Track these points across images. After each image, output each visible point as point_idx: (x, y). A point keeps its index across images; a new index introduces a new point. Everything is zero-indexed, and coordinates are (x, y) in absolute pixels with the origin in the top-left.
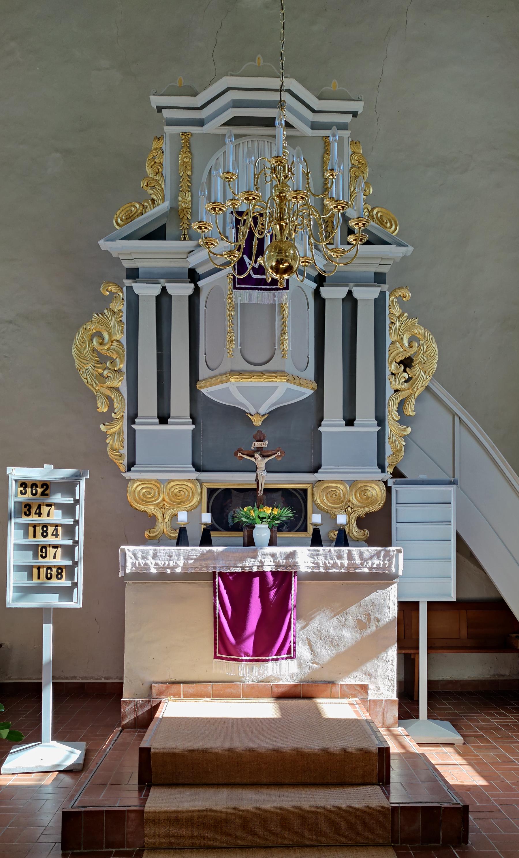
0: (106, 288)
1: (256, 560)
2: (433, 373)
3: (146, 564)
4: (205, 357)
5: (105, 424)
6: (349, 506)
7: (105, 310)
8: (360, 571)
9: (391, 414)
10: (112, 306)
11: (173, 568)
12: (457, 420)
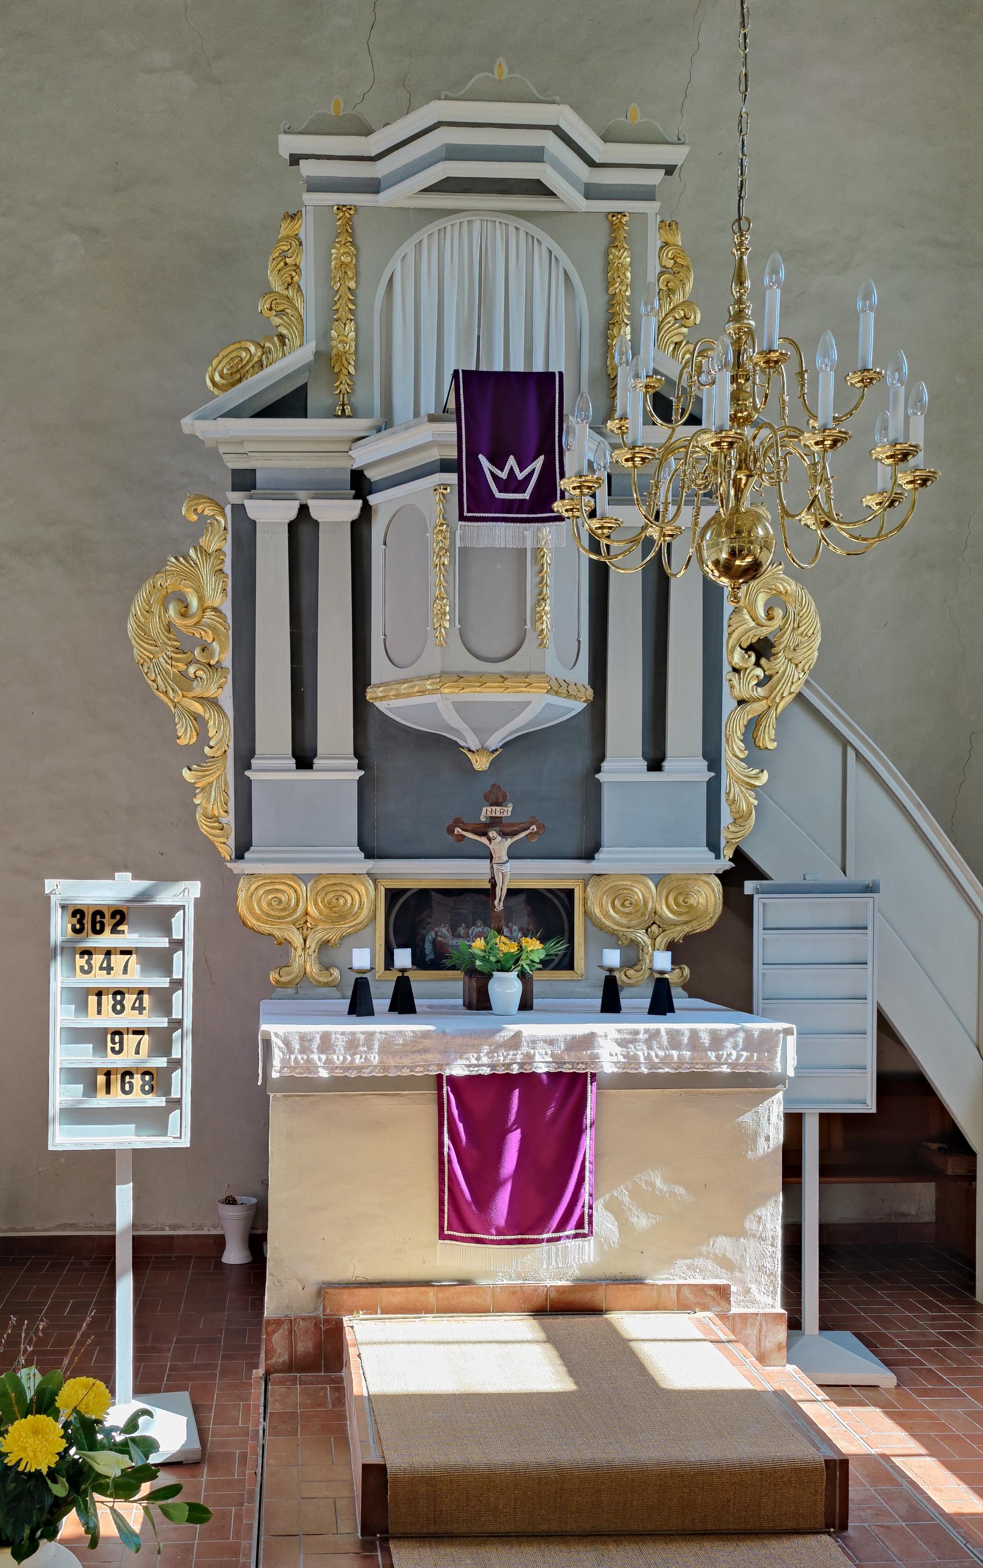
0: (193, 508)
1: (519, 1052)
2: (811, 667)
3: (309, 1061)
4: (385, 639)
5: (192, 768)
6: (654, 923)
7: (191, 551)
8: (717, 1070)
9: (733, 748)
10: (203, 541)
11: (360, 1069)
12: (851, 753)
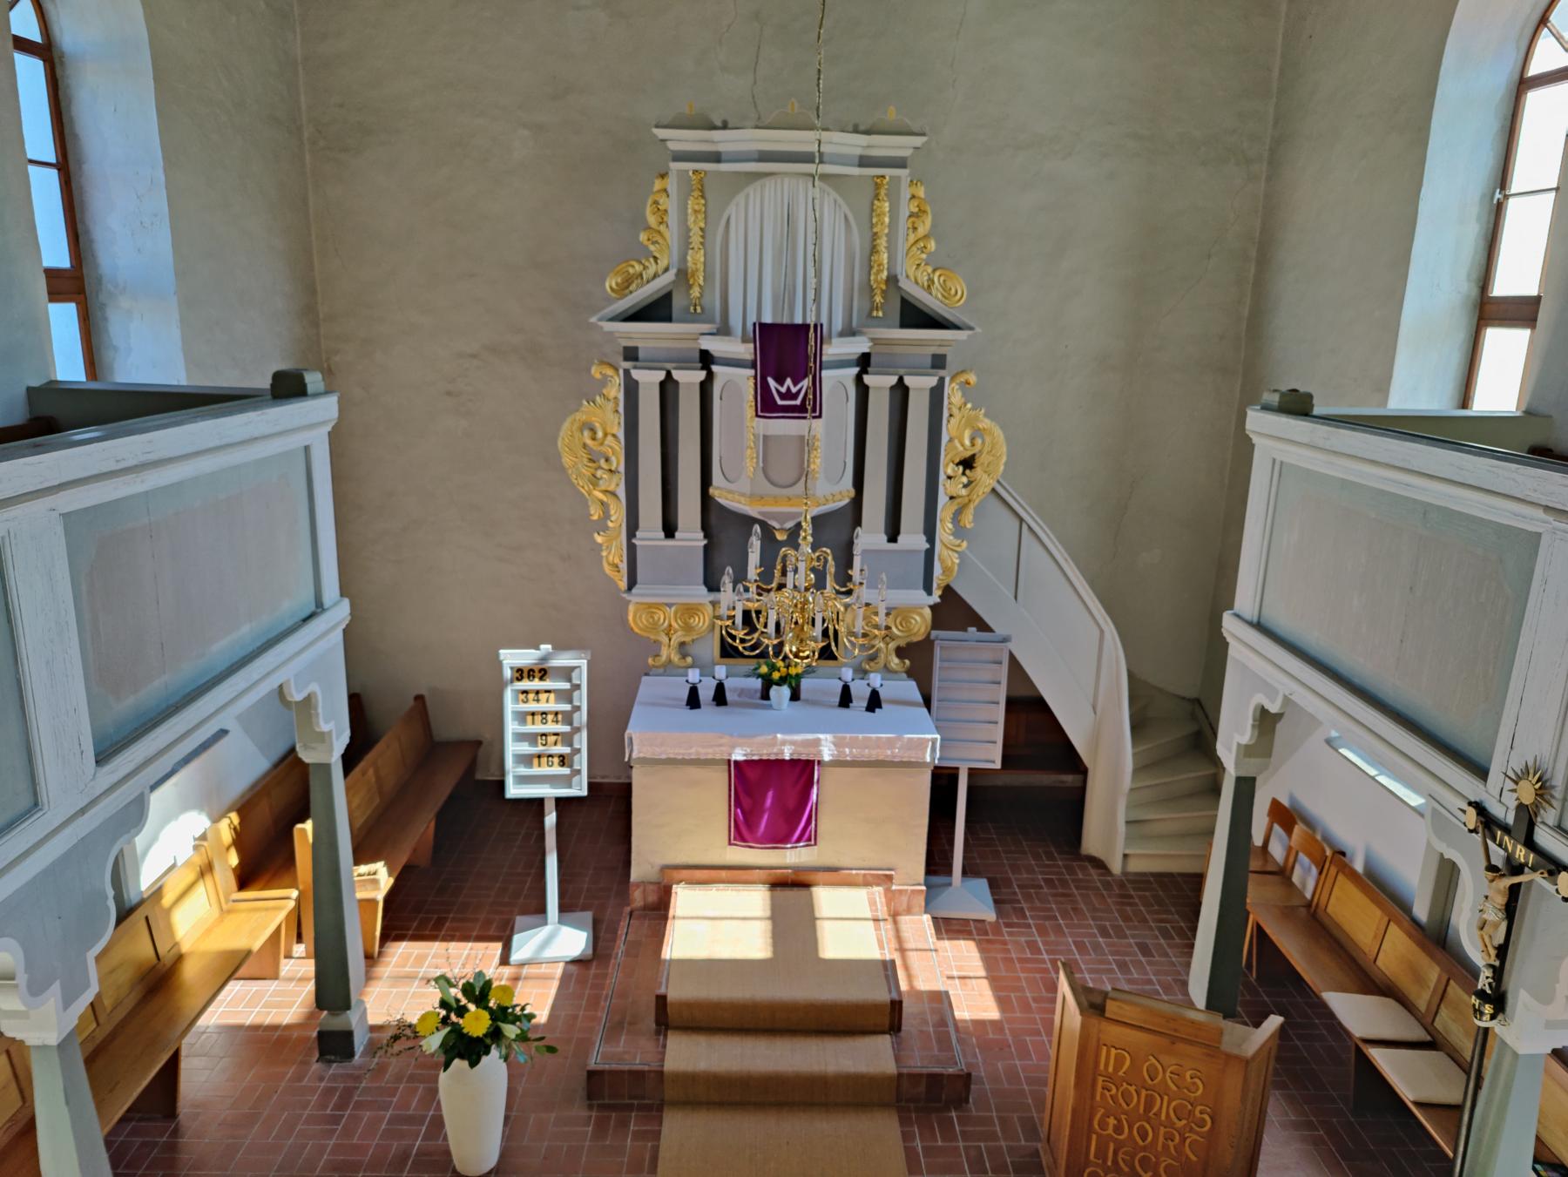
12: (1025, 527)
